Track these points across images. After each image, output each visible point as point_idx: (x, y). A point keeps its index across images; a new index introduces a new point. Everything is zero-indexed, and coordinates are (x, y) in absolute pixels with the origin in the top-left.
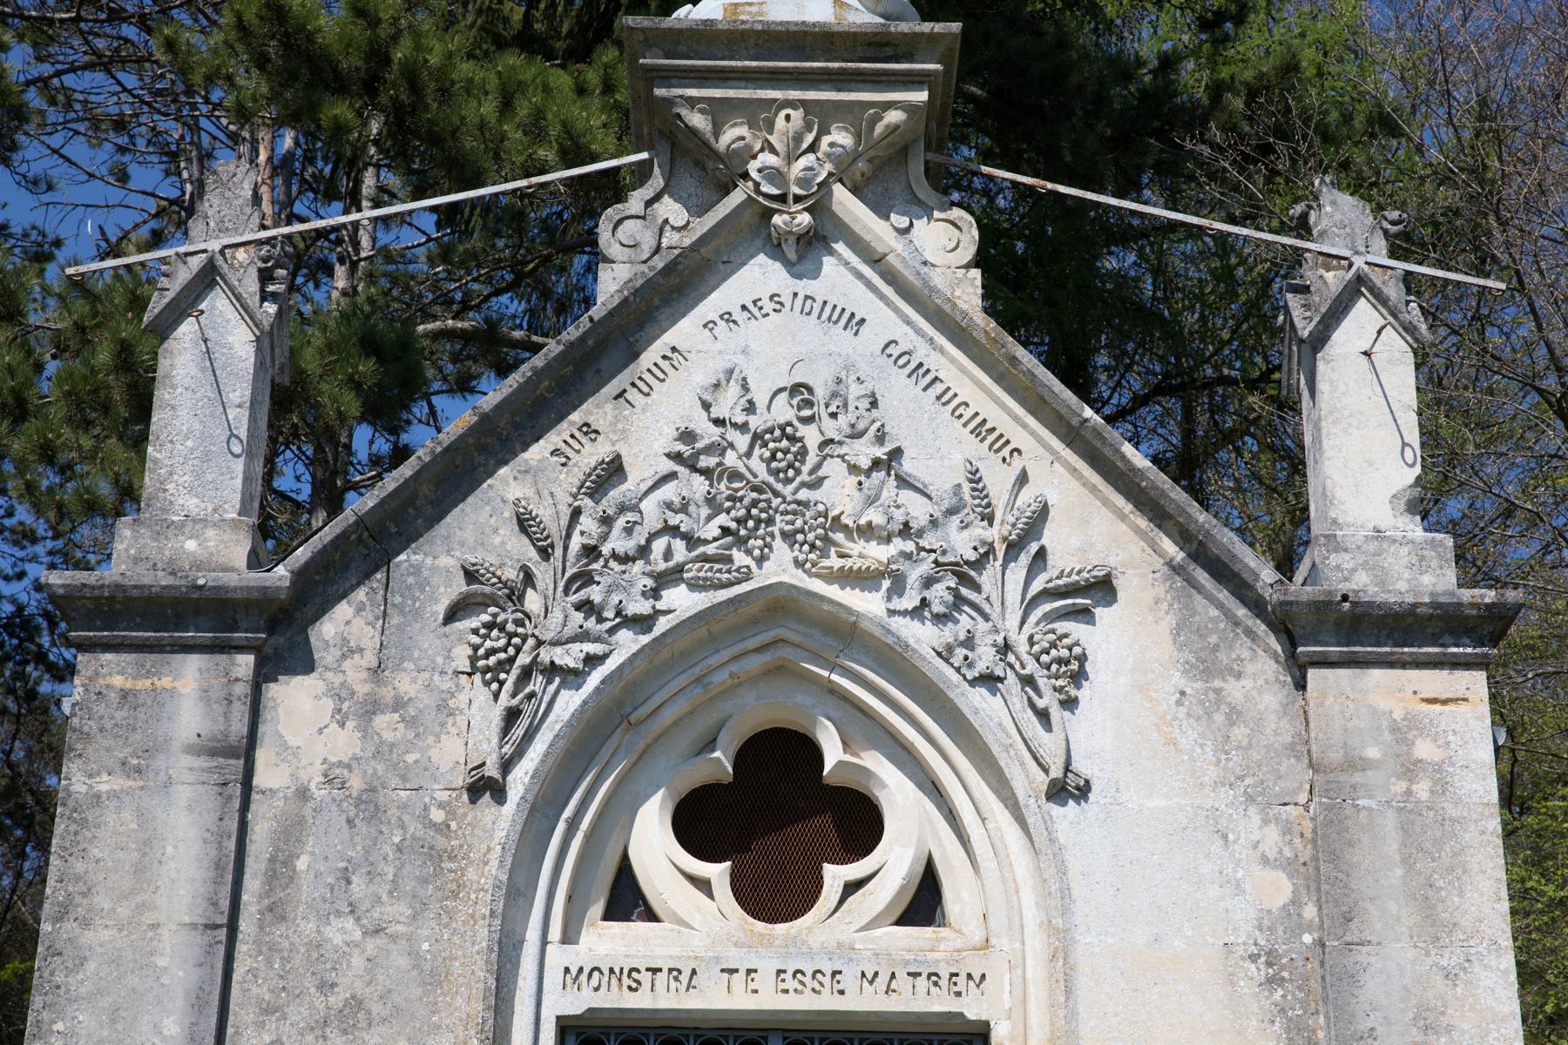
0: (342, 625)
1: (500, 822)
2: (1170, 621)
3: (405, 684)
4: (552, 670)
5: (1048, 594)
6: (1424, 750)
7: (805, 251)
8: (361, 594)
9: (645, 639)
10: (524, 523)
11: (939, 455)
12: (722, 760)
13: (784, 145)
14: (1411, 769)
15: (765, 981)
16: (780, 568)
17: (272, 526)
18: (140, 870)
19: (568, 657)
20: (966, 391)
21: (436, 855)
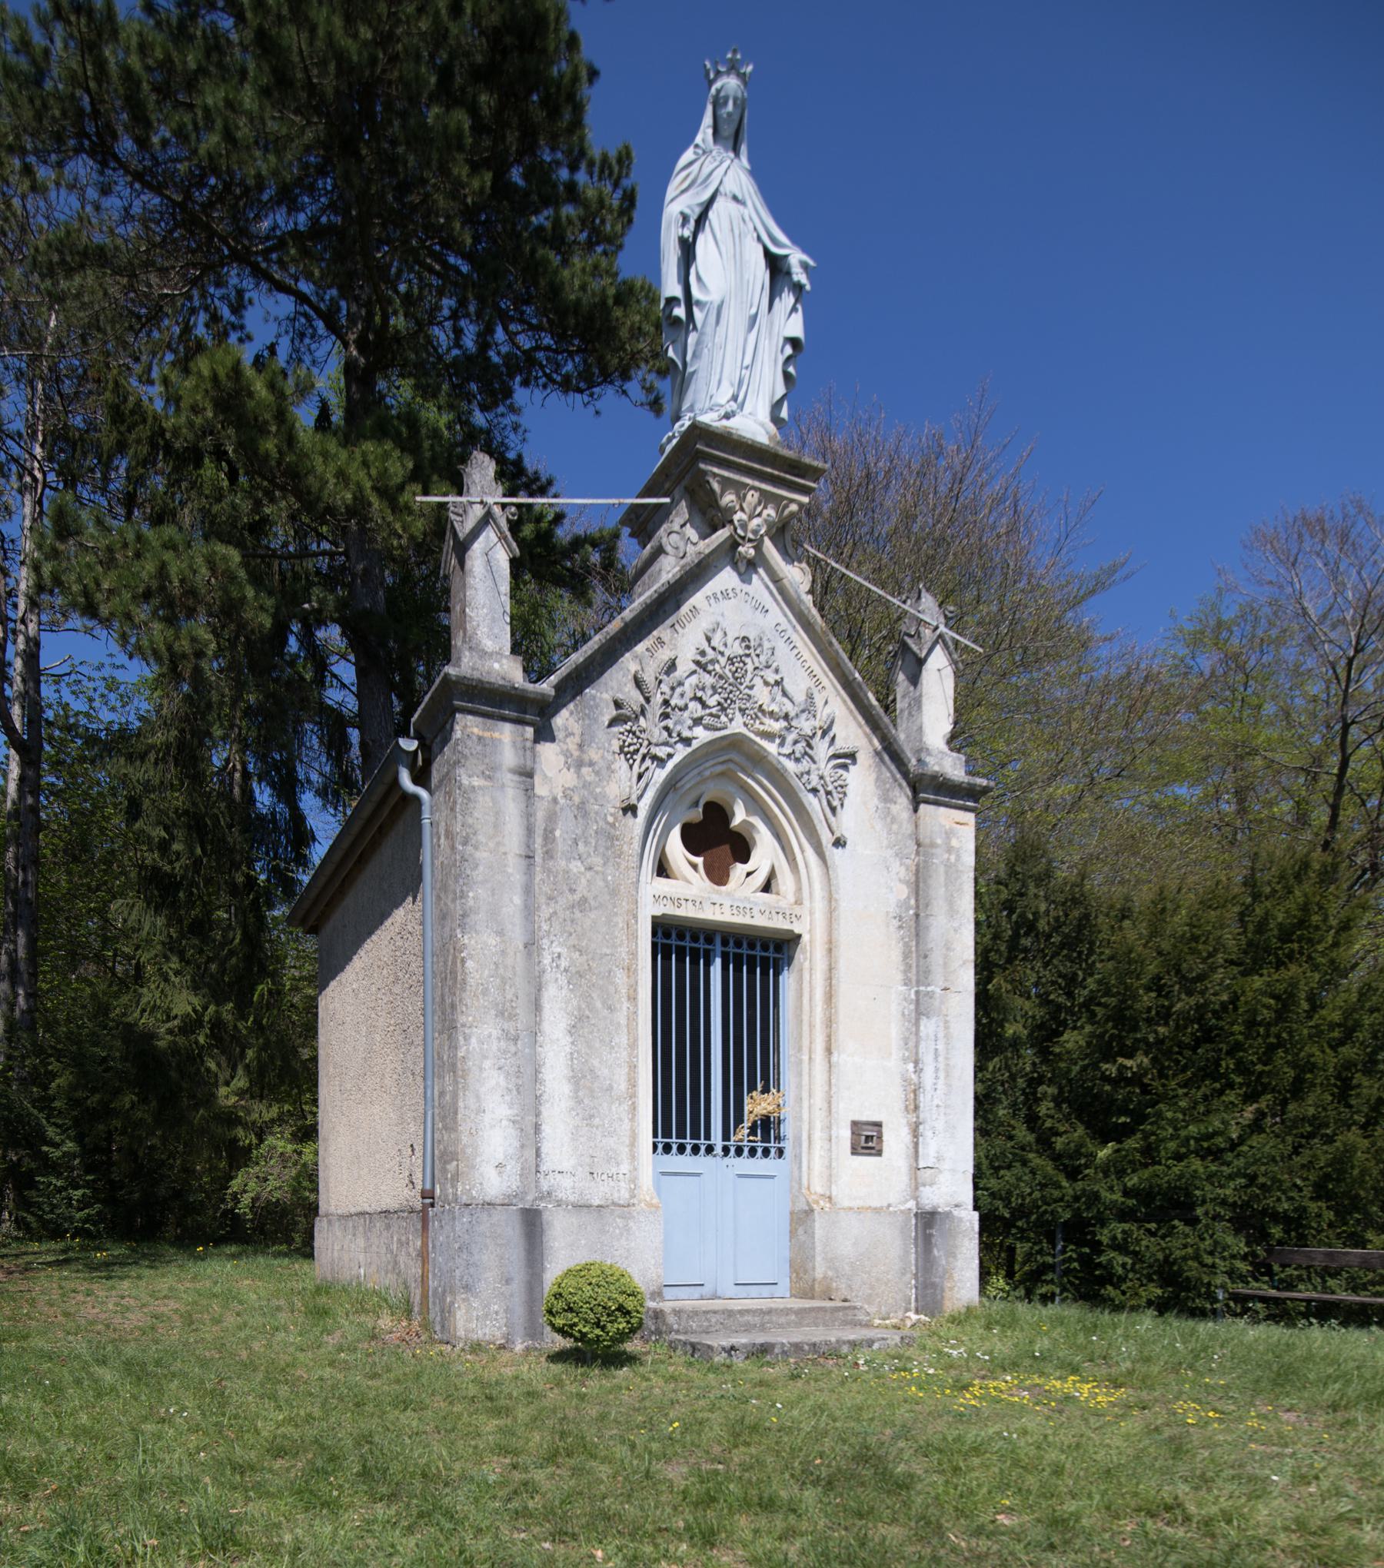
2: (874, 776)
3: (593, 754)
4: (654, 758)
5: (835, 756)
6: (954, 843)
8: (571, 706)
9: (689, 750)
10: (638, 683)
11: (798, 685)
14: (950, 850)
15: (726, 909)
16: (737, 726)
18: (496, 826)
19: (662, 752)
20: (806, 655)
21: (610, 837)
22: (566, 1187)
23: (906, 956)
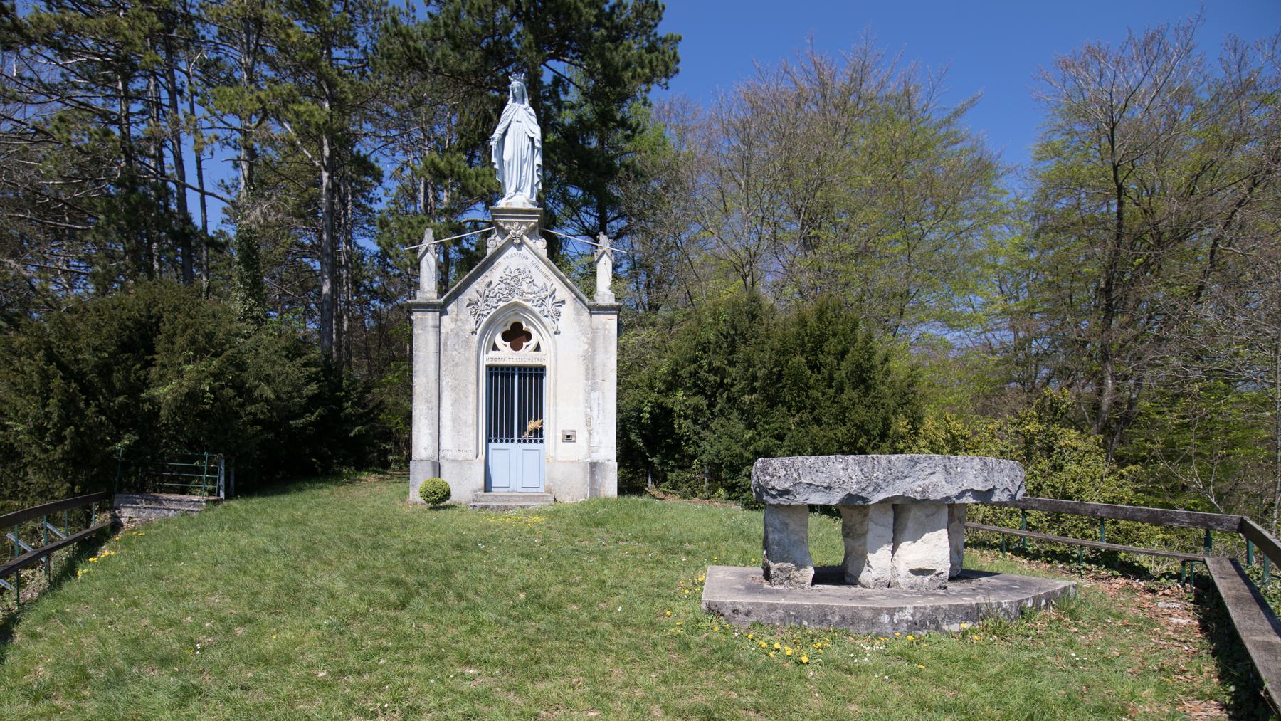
0: (451, 308)
1: (476, 337)
7: (519, 246)
11: (540, 281)
12: (508, 328)
13: (516, 228)
16: (516, 299)
17: (441, 293)
21: (467, 342)
22: (449, 455)
23: (587, 369)
